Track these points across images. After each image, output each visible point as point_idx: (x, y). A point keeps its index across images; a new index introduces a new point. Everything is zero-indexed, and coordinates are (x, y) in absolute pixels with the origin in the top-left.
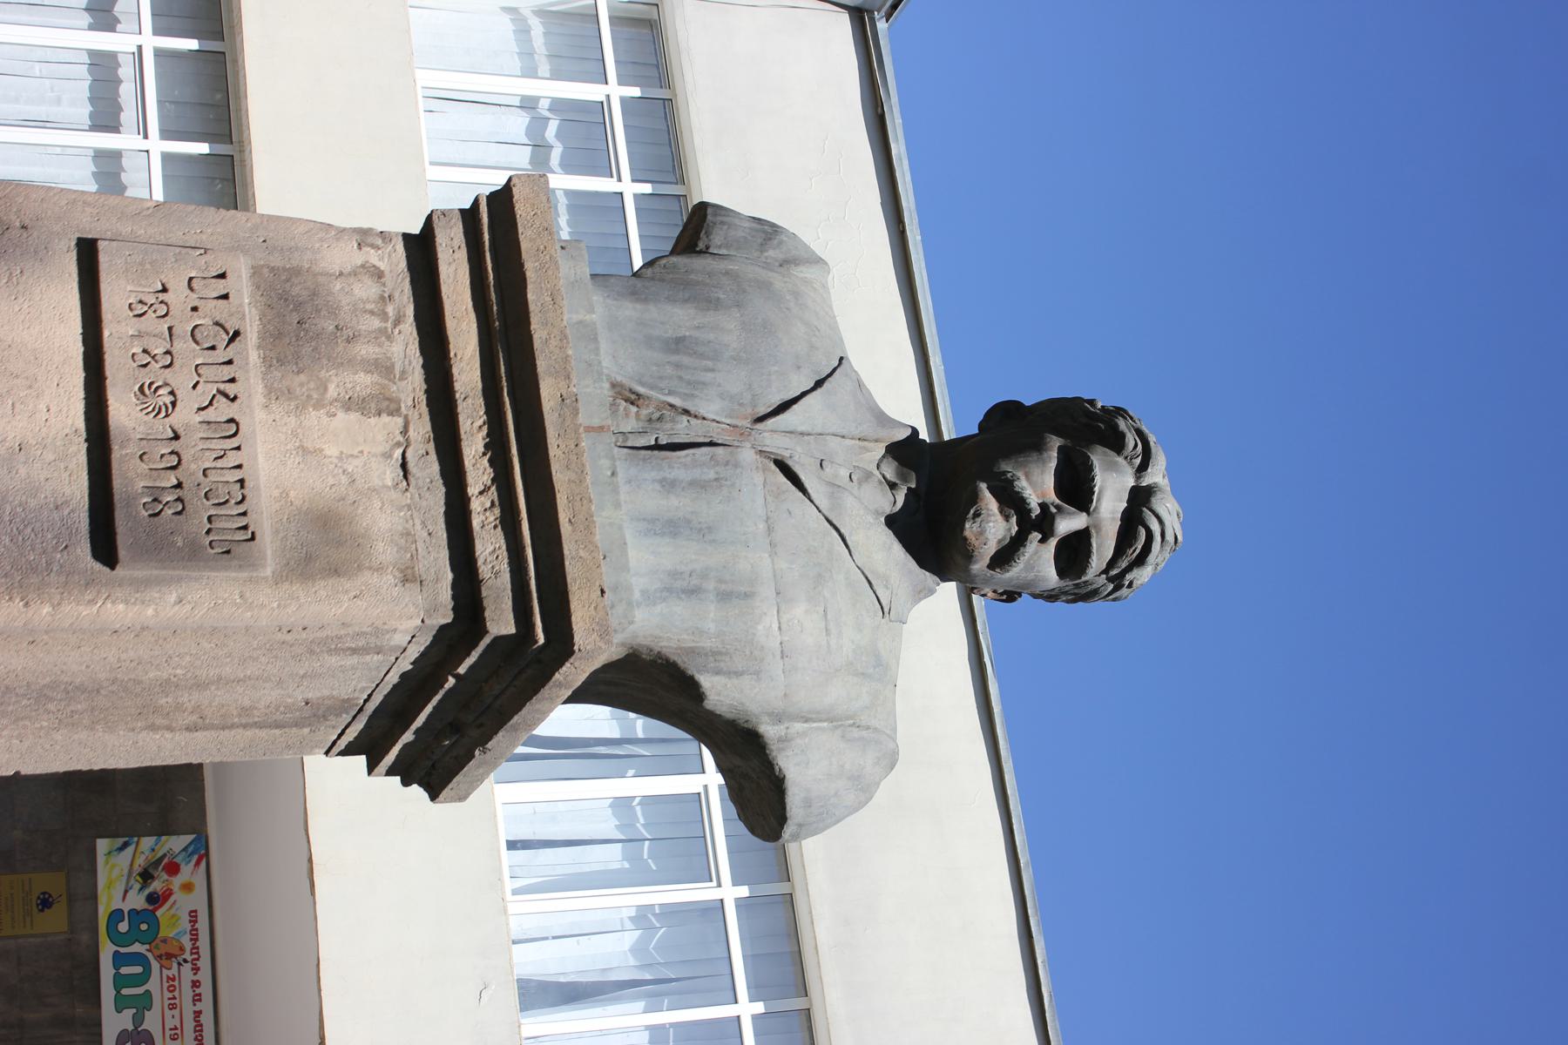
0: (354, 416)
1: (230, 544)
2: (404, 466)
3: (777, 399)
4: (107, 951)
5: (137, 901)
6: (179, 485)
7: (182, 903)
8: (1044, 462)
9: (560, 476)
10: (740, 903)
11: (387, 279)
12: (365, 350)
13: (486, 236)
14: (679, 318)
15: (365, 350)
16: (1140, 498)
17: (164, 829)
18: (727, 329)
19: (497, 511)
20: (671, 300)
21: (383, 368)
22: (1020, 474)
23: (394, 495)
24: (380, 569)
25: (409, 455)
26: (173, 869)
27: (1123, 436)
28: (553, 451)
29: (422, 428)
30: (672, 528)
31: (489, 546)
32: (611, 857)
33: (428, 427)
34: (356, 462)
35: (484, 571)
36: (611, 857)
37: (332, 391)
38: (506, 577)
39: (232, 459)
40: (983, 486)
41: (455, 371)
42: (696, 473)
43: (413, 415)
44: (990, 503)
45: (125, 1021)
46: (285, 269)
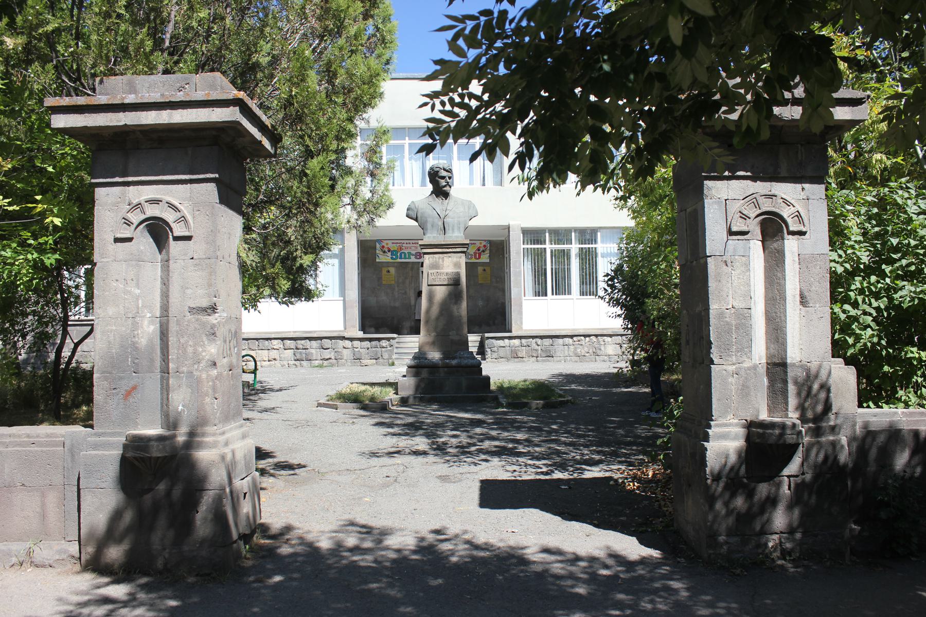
5: (389, 254)
7: (390, 245)
14: (429, 226)
16: (444, 169)
17: (375, 248)
18: (430, 220)
26: (383, 247)
30: (453, 230)
45: (413, 257)
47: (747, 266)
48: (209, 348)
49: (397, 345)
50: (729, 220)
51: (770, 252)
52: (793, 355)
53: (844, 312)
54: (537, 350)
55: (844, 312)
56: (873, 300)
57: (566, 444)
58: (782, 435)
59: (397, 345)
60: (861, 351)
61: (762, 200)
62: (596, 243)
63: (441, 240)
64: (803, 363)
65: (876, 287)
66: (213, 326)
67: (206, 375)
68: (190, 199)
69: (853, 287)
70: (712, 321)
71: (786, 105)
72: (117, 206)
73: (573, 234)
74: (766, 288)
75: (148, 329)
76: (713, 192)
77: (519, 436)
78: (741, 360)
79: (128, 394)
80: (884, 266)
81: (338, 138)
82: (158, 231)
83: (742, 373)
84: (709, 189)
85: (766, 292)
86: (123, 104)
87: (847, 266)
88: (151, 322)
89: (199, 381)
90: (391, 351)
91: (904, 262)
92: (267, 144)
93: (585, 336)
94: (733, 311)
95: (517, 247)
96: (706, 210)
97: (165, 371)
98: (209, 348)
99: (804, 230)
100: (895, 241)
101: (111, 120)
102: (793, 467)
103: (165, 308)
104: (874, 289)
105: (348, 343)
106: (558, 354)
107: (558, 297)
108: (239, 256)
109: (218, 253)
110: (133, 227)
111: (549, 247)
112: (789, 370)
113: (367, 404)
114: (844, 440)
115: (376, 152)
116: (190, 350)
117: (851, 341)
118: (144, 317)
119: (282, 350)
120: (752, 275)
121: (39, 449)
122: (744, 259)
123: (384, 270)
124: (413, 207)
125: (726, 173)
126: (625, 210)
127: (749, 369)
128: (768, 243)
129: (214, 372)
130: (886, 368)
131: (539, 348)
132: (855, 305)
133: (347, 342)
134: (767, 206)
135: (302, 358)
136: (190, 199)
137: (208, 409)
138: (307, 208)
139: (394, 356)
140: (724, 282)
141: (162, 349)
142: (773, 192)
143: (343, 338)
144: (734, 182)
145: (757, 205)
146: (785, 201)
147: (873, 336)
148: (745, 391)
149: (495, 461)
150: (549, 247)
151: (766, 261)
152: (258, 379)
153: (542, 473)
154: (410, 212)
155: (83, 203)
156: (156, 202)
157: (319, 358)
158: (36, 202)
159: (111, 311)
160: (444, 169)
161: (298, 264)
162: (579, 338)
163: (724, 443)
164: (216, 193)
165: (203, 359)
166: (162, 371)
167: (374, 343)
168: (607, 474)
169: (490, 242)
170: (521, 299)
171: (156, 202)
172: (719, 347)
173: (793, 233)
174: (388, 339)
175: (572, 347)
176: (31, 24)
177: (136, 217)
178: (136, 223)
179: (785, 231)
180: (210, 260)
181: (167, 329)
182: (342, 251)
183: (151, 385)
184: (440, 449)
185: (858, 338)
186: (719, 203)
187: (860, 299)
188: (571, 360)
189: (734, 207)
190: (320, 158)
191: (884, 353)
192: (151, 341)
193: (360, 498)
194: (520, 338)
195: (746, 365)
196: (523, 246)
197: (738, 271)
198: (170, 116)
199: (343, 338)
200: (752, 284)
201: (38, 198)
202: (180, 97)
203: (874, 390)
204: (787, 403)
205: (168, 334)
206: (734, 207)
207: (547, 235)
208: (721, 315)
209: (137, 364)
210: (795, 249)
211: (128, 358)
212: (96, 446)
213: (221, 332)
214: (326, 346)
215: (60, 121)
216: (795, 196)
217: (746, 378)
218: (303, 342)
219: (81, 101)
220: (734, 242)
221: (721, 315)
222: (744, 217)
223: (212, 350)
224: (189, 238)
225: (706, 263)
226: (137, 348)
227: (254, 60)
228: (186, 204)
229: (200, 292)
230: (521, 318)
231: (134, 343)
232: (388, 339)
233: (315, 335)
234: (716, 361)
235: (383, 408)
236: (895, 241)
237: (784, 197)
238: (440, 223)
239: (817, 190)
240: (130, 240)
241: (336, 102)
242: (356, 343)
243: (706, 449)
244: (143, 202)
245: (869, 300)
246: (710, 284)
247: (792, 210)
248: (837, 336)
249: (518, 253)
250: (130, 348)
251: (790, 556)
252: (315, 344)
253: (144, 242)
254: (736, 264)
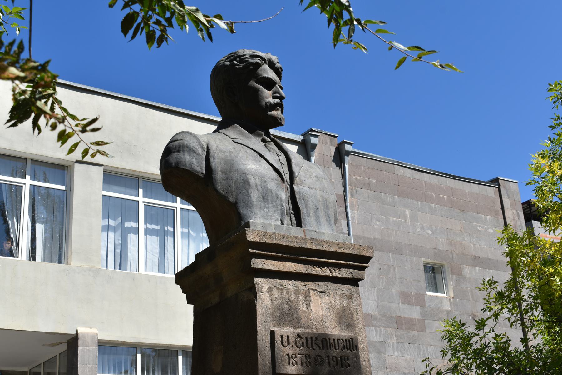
0: (311, 304)
2: (321, 292)
3: (274, 173)
6: (341, 357)
8: (262, 91)
9: (333, 249)
10: (34, 178)
11: (271, 286)
12: (293, 297)
13: (262, 252)
15: (293, 297)
19: (336, 269)
20: (249, 196)
21: (297, 292)
22: (267, 100)
23: (331, 297)
24: (350, 305)
25: (319, 290)
27: (257, 63)
28: (326, 249)
29: (311, 285)
30: (317, 218)
33: (311, 283)
34: (323, 305)
35: (350, 276)
37: (305, 309)
38: (352, 271)
39: (332, 342)
40: (269, 113)
41: (299, 272)
42: (304, 205)
43: (308, 287)
44: (274, 113)
46: (272, 317)
73: (180, 358)
207: (139, 356)
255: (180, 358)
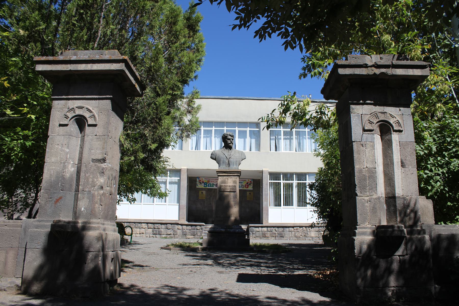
1: (235, 186)
4: (208, 187)
7: (204, 180)
14: (221, 162)
16: (230, 135)
17: (196, 181)
18: (222, 159)
26: (200, 180)
30: (233, 164)
31: (235, 174)
32: (208, 139)
36: (208, 139)
47: (373, 147)
48: (100, 179)
49: (205, 229)
50: (363, 124)
51: (385, 141)
52: (399, 192)
53: (426, 174)
54: (275, 234)
55: (426, 174)
56: (440, 169)
57: (286, 264)
58: (394, 231)
59: (205, 229)
60: (435, 193)
61: (379, 115)
62: (306, 180)
63: (227, 169)
64: (404, 196)
65: (441, 162)
66: (103, 169)
67: (97, 193)
68: (98, 107)
69: (429, 162)
70: (356, 174)
71: (389, 68)
72: (62, 109)
73: (294, 176)
74: (383, 159)
75: (71, 169)
76: (355, 110)
77: (261, 261)
78: (372, 194)
79: (57, 201)
80: (444, 153)
81: (173, 89)
82: (81, 122)
83: (372, 201)
84: (353, 109)
85: (383, 161)
86: (70, 60)
87: (426, 152)
88: (73, 166)
89: (93, 196)
90: (202, 232)
91: (454, 150)
92: (138, 89)
93: (300, 227)
94: (367, 169)
95: (267, 181)
96: (352, 119)
97: (77, 190)
98: (100, 179)
99: (401, 129)
100: (449, 140)
101: (64, 68)
102: (400, 252)
103: (80, 160)
104: (440, 163)
105: (180, 227)
106: (286, 236)
107: (287, 207)
108: (120, 141)
109: (109, 134)
110: (69, 119)
111: (282, 182)
112: (397, 200)
113: (187, 249)
114: (427, 237)
115: (192, 102)
116: (90, 180)
117: (430, 188)
118: (69, 163)
119: (147, 229)
120: (376, 152)
121: (8, 228)
122: (371, 143)
123: (200, 192)
124: (214, 153)
125: (361, 102)
126: (319, 157)
127: (376, 199)
128: (383, 137)
129: (102, 192)
130: (449, 203)
131: (277, 232)
132: (431, 171)
133: (180, 226)
134: (382, 117)
135: (157, 233)
136: (98, 107)
137: (97, 210)
138: (155, 121)
139: (203, 234)
140: (362, 155)
141: (77, 180)
142: (385, 111)
143: (178, 224)
144: (365, 106)
145: (377, 117)
146: (391, 115)
147: (441, 185)
148: (374, 210)
149: (249, 268)
150: (282, 182)
151: (383, 145)
152: (133, 240)
153: (272, 273)
154: (213, 156)
155: (47, 112)
156: (81, 108)
157: (165, 233)
158: (24, 107)
159: (53, 160)
160: (230, 135)
161: (149, 148)
162: (297, 228)
163: (363, 238)
164: (111, 105)
165: (96, 185)
166: (76, 191)
167: (193, 227)
168: (306, 273)
169: (253, 180)
170: (268, 207)
171: (81, 108)
172: (360, 187)
173: (396, 131)
174: (200, 225)
175: (293, 232)
176: (33, 25)
177: (70, 115)
178: (70, 117)
179: (392, 130)
180: (106, 137)
181: (80, 170)
182: (179, 180)
183: (69, 197)
184: (219, 264)
185: (433, 187)
186: (358, 116)
187: (433, 168)
188: (293, 239)
189: (366, 118)
190: (163, 97)
191: (447, 195)
192: (72, 175)
193: (175, 278)
194: (267, 227)
195: (374, 197)
196: (269, 181)
197: (369, 150)
198: (92, 67)
199: (178, 224)
200: (376, 155)
201: (25, 105)
202: (97, 57)
203: (442, 215)
204: (397, 218)
205: (80, 172)
206: (366, 118)
207: (282, 176)
208: (360, 171)
209: (63, 186)
210: (397, 139)
211: (60, 183)
212: (37, 227)
213: (107, 173)
214: (169, 228)
215: (39, 68)
216: (396, 113)
217: (374, 204)
218: (157, 225)
219: (51, 58)
220: (366, 135)
221: (360, 171)
222: (371, 123)
223: (102, 180)
224: (95, 125)
225: (352, 145)
226: (64, 178)
227: (136, 54)
228: (96, 109)
229: (98, 151)
230: (268, 217)
231: (63, 176)
232: (200, 225)
233: (164, 222)
234: (358, 194)
235: (195, 250)
236: (449, 140)
237: (391, 113)
238: (227, 161)
239: (408, 111)
240: (66, 125)
241: (172, 73)
242: (184, 227)
243: (354, 240)
244: (75, 108)
245: (438, 169)
246: (354, 156)
247: (395, 119)
248: (422, 186)
249: (267, 184)
250: (60, 178)
251: (402, 299)
252: (163, 226)
253: (74, 127)
254: (368, 146)
255: (294, 176)
